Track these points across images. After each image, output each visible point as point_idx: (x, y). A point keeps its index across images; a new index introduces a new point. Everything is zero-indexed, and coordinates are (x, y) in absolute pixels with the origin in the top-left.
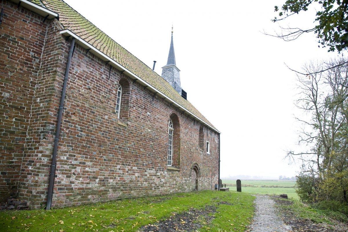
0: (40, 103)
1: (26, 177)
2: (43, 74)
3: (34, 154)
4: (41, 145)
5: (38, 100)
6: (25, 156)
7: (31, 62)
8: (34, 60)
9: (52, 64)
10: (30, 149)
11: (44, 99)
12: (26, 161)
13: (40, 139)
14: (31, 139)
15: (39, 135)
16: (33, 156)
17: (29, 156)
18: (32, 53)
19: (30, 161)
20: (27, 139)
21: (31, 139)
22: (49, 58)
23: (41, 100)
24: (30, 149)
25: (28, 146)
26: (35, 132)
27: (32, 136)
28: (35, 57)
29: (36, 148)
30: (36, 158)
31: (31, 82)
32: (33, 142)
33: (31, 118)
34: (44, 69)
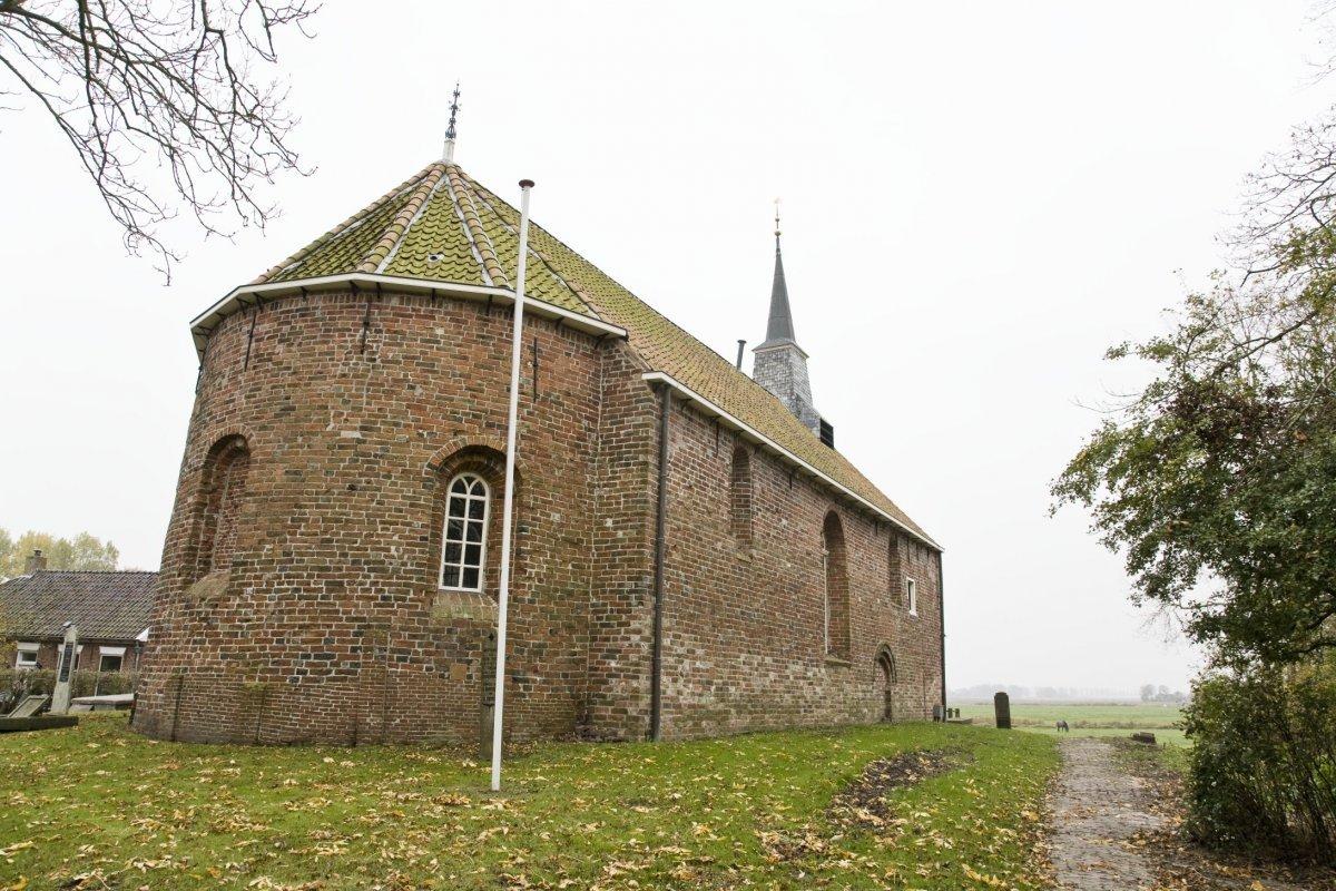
0: (616, 529)
1: (605, 682)
2: (612, 466)
3: (619, 636)
4: (635, 618)
5: (609, 523)
6: (594, 639)
7: (585, 441)
8: (590, 436)
9: (632, 446)
10: (603, 625)
11: (623, 521)
12: (600, 650)
13: (629, 605)
14: (605, 605)
15: (628, 598)
16: (615, 639)
17: (607, 639)
18: (585, 423)
19: (608, 651)
20: (593, 605)
21: (605, 605)
22: (622, 432)
23: (614, 522)
24: (603, 625)
25: (599, 618)
26: (611, 592)
27: (606, 598)
28: (590, 430)
29: (620, 624)
30: (626, 643)
31: (589, 485)
32: (612, 611)
33: (596, 561)
34: (611, 454)
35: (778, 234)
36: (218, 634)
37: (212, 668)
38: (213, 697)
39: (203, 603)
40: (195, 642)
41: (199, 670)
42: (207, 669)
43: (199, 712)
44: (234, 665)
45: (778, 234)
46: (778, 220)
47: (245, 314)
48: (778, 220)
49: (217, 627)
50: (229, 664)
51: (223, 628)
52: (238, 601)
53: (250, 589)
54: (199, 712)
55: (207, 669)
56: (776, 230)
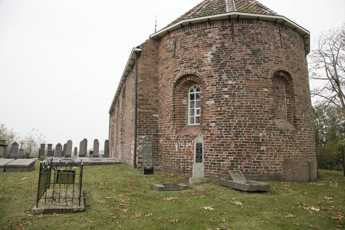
35: (156, 26)
36: (297, 144)
37: (298, 156)
38: (301, 165)
39: (289, 132)
40: (290, 146)
41: (294, 156)
42: (297, 156)
43: (298, 171)
44: (303, 154)
45: (156, 26)
46: (156, 22)
47: (275, 25)
48: (156, 22)
49: (296, 141)
50: (302, 154)
51: (298, 142)
52: (300, 133)
53: (303, 129)
54: (298, 171)
55: (297, 156)
56: (155, 24)
